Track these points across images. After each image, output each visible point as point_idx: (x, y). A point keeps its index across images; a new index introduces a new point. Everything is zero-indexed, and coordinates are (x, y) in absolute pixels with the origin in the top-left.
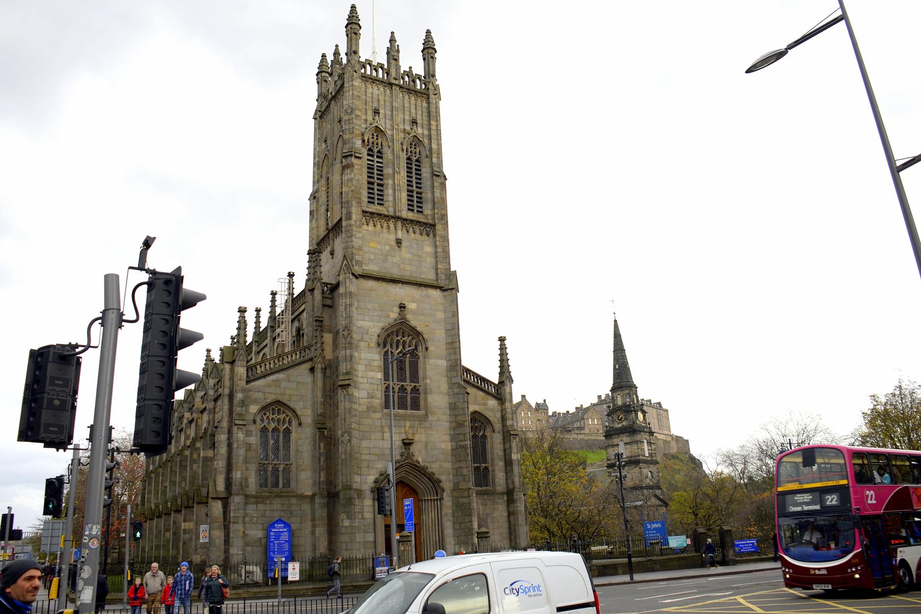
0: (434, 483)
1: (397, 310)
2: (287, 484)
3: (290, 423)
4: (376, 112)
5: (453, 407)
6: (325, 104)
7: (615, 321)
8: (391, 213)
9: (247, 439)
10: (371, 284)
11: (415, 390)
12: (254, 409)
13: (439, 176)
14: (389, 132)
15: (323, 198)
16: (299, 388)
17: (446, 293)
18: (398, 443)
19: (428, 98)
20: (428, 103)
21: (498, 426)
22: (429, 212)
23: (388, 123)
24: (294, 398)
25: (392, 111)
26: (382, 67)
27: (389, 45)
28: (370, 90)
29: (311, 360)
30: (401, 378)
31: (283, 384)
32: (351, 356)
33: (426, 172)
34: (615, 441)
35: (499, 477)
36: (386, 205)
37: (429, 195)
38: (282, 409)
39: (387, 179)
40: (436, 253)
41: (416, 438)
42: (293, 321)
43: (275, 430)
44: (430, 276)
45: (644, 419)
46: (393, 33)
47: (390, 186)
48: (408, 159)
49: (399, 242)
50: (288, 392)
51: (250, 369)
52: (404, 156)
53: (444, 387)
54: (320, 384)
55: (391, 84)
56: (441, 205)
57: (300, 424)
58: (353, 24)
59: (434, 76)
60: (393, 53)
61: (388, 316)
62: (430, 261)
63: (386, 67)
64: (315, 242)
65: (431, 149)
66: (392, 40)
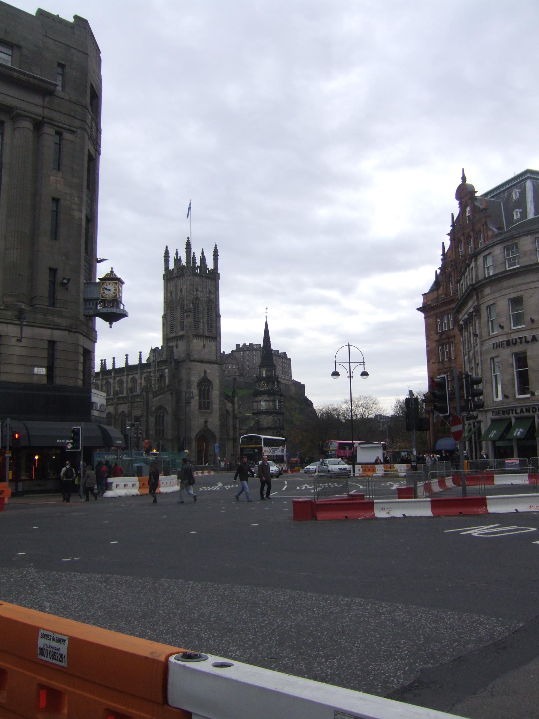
0: (214, 436)
2: (163, 435)
5: (220, 409)
7: (266, 322)
9: (152, 419)
10: (196, 363)
11: (208, 403)
12: (154, 409)
15: (169, 318)
16: (167, 401)
18: (203, 422)
21: (231, 413)
22: (215, 332)
23: (201, 294)
28: (195, 280)
30: (204, 399)
33: (214, 315)
34: (259, 399)
35: (231, 432)
41: (209, 420)
42: (158, 370)
43: (160, 416)
44: (213, 358)
45: (278, 386)
48: (208, 309)
49: (204, 346)
51: (153, 393)
52: (206, 308)
53: (218, 402)
55: (202, 276)
60: (203, 259)
62: (214, 352)
66: (203, 253)
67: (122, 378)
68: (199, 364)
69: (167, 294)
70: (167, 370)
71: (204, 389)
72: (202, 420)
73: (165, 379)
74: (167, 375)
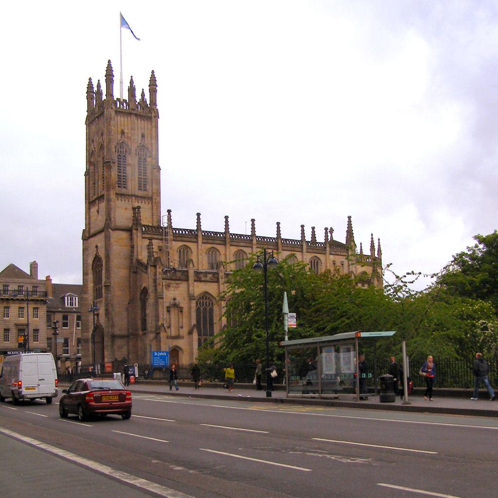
6: (93, 118)
26: (125, 101)
40: (153, 214)
46: (132, 77)
48: (139, 158)
59: (155, 104)
60: (132, 90)
63: (128, 102)
66: (132, 82)
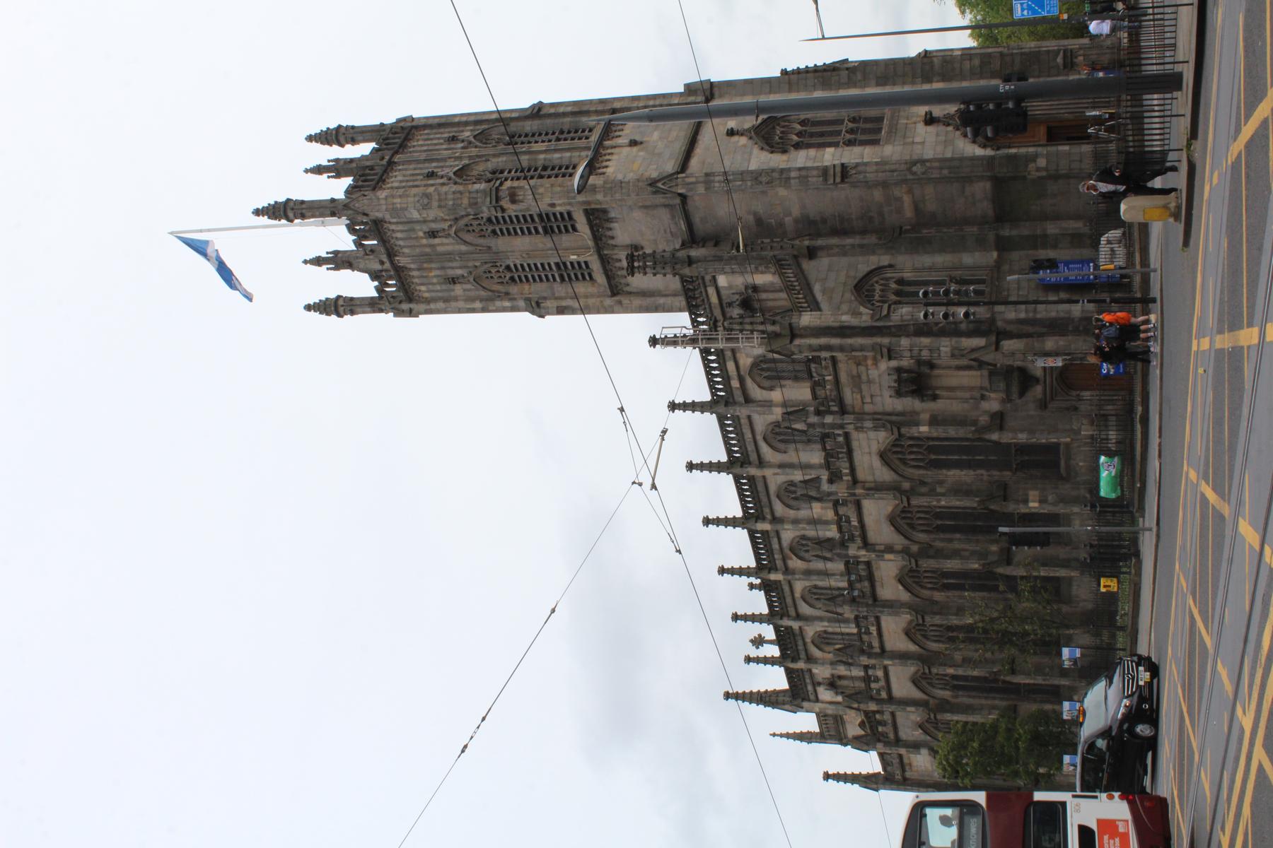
1: (736, 138)
3: (887, 279)
4: (431, 175)
8: (590, 153)
10: (694, 162)
13: (538, 111)
14: (466, 162)
17: (716, 93)
18: (931, 129)
19: (416, 128)
20: (425, 127)
24: (852, 274)
25: (432, 160)
27: (325, 176)
29: (795, 257)
30: (839, 133)
31: (830, 284)
32: (800, 169)
33: (529, 126)
36: (575, 160)
37: (567, 120)
38: (867, 287)
39: (536, 160)
47: (548, 156)
49: (633, 143)
50: (842, 278)
54: (834, 241)
55: (391, 163)
56: (581, 109)
57: (891, 266)
58: (285, 211)
60: (337, 169)
61: (744, 146)
64: (608, 302)
65: (496, 120)
67: (773, 489)
68: (699, 151)
69: (456, 299)
70: (722, 281)
71: (799, 134)
72: (924, 133)
73: (755, 288)
74: (739, 281)
